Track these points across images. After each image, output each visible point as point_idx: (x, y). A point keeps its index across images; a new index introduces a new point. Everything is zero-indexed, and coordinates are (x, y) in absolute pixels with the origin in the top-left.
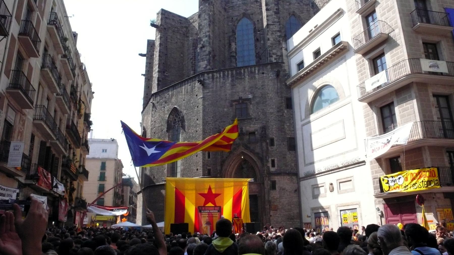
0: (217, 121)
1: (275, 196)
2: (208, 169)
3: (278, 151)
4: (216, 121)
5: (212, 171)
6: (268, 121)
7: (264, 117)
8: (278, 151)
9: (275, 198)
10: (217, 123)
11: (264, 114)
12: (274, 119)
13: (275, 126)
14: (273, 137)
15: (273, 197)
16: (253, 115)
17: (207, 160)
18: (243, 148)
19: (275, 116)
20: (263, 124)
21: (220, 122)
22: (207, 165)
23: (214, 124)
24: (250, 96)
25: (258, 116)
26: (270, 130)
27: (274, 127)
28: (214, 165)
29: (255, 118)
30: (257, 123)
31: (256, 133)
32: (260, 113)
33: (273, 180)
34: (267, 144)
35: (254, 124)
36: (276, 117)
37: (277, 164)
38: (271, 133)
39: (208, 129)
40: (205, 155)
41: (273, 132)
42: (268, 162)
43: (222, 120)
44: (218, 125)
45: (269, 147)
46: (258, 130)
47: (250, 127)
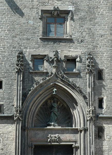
10: (16, 39)
11: (90, 36)
19: (106, 40)
24: (71, 8)
32: (84, 34)
33: (100, 125)
36: (108, 42)
37: (107, 105)
41: (103, 62)
44: (19, 43)
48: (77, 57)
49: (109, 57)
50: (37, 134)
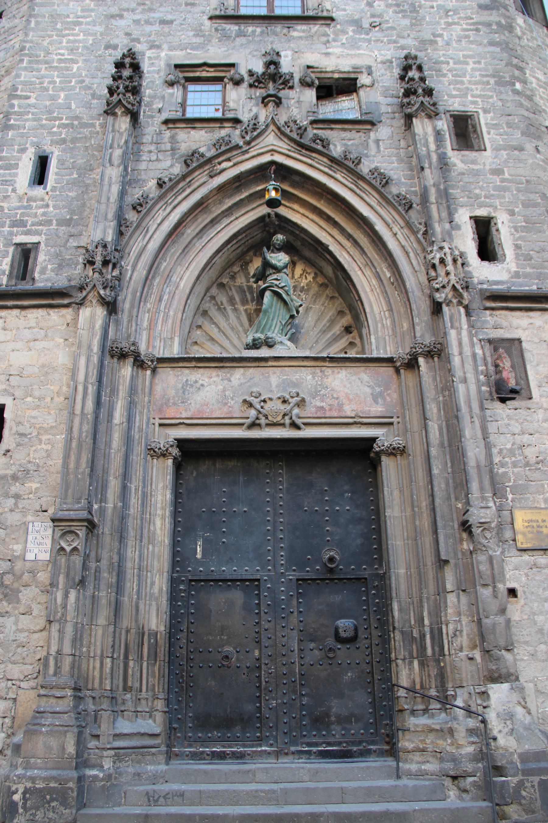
0: (121, 17)
1: (526, 439)
2: (17, 245)
3: (506, 176)
4: (112, 16)
5: (42, 257)
6: (436, 42)
7: (407, 22)
8: (506, 176)
9: (531, 453)
12: (467, 37)
13: (475, 63)
14: (471, 108)
15: (512, 452)
16: (345, 10)
17: (20, 199)
18: (283, 145)
20: (403, 48)
21: (137, 22)
22: (14, 224)
23: (99, 29)
25: (373, 16)
26: (444, 75)
27: (469, 68)
28: (62, 222)
29: (357, 23)
30: (369, 41)
31: (364, 79)
34: (438, 134)
35: (353, 44)
36: (477, 30)
37: (517, 247)
38: (459, 90)
39: (59, 49)
40: (16, 166)
42: (458, 227)
43: (156, 15)
44: (128, 34)
45: (450, 153)
46: (376, 74)
47: (327, 54)
48: (357, 70)
49: (487, 76)
50: (192, 386)
